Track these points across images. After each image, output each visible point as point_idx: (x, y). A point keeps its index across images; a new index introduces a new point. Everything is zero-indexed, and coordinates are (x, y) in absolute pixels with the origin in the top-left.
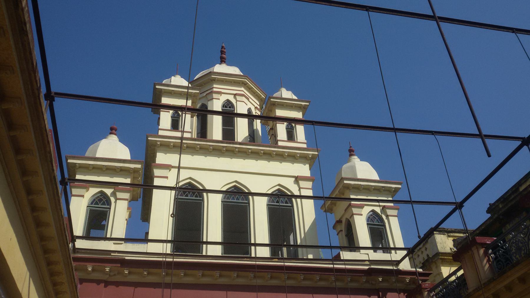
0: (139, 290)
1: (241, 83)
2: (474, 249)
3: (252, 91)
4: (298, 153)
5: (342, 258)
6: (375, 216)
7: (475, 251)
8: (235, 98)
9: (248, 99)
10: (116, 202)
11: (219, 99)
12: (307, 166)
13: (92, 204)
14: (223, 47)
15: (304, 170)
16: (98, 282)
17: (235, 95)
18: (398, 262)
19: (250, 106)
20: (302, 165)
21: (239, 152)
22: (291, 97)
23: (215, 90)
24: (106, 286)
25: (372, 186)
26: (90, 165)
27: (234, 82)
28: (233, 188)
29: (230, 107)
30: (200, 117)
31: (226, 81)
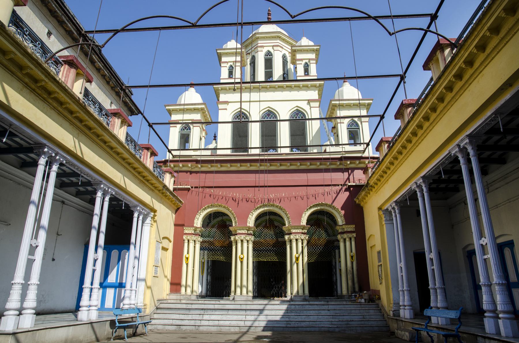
0: (208, 175)
1: (277, 37)
2: (383, 144)
3: (285, 41)
4: (309, 84)
5: (327, 151)
6: (354, 123)
7: (383, 146)
8: (273, 48)
9: (282, 48)
10: (193, 128)
11: (262, 51)
12: (317, 92)
13: (181, 130)
14: (269, 10)
15: (314, 94)
16: (186, 172)
17: (273, 46)
18: (364, 151)
19: (284, 52)
20: (313, 92)
21: (270, 87)
22: (307, 44)
23: (259, 45)
24: (191, 174)
25: (351, 103)
26: (177, 109)
27: (272, 37)
28: (267, 112)
29: (270, 56)
30: (252, 65)
31: (266, 38)
